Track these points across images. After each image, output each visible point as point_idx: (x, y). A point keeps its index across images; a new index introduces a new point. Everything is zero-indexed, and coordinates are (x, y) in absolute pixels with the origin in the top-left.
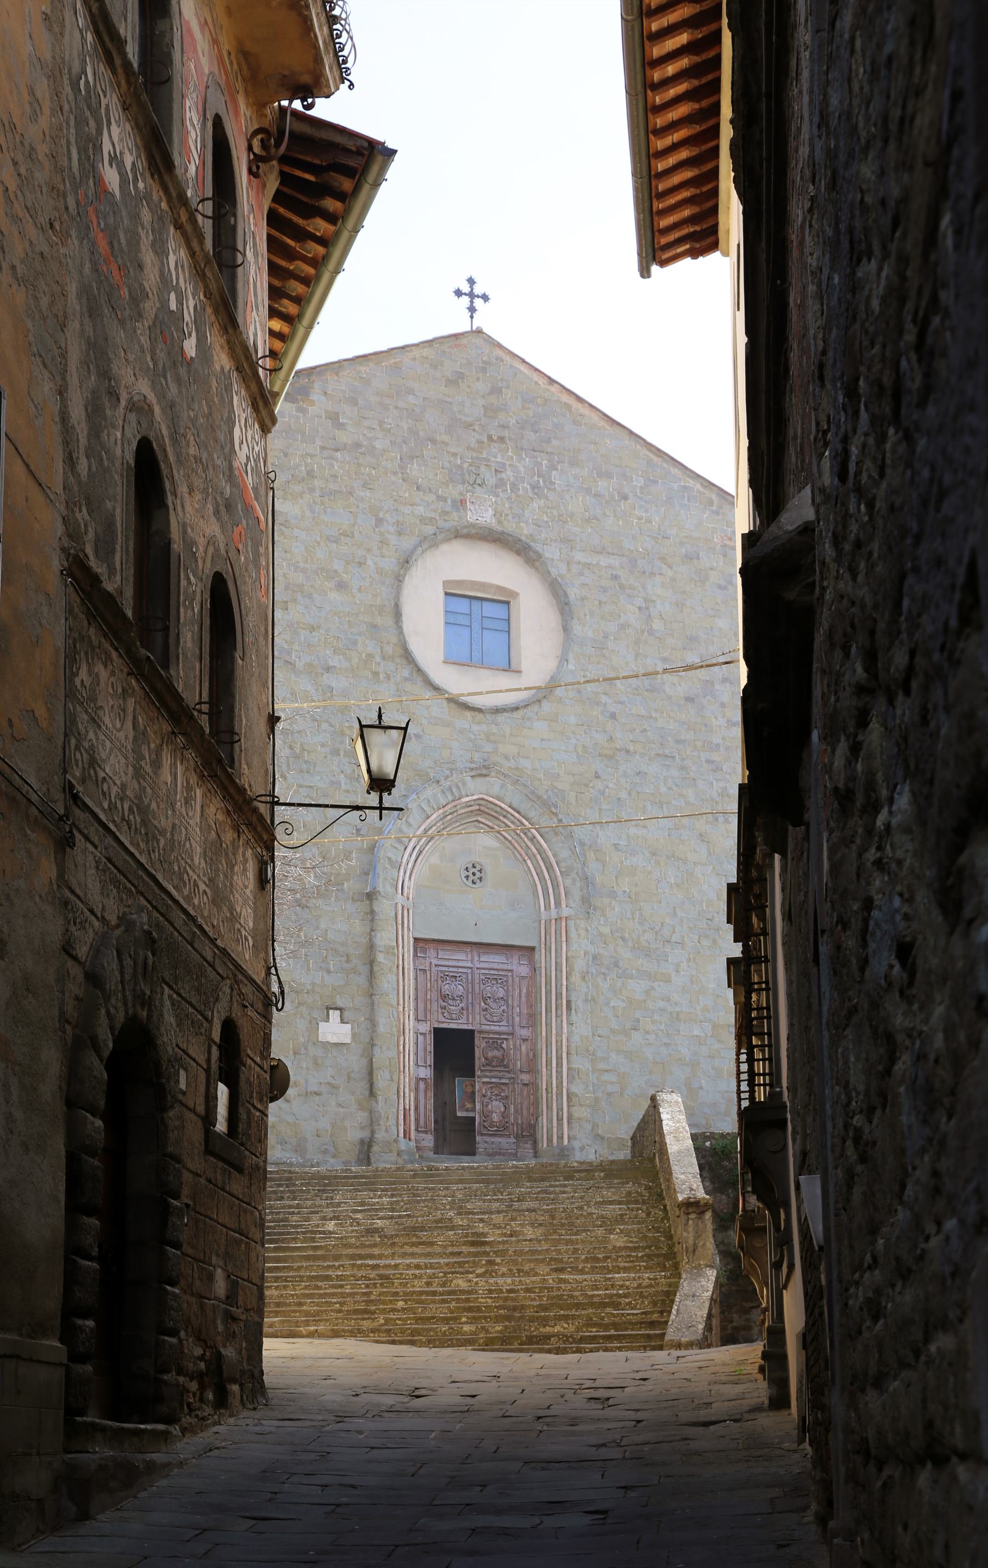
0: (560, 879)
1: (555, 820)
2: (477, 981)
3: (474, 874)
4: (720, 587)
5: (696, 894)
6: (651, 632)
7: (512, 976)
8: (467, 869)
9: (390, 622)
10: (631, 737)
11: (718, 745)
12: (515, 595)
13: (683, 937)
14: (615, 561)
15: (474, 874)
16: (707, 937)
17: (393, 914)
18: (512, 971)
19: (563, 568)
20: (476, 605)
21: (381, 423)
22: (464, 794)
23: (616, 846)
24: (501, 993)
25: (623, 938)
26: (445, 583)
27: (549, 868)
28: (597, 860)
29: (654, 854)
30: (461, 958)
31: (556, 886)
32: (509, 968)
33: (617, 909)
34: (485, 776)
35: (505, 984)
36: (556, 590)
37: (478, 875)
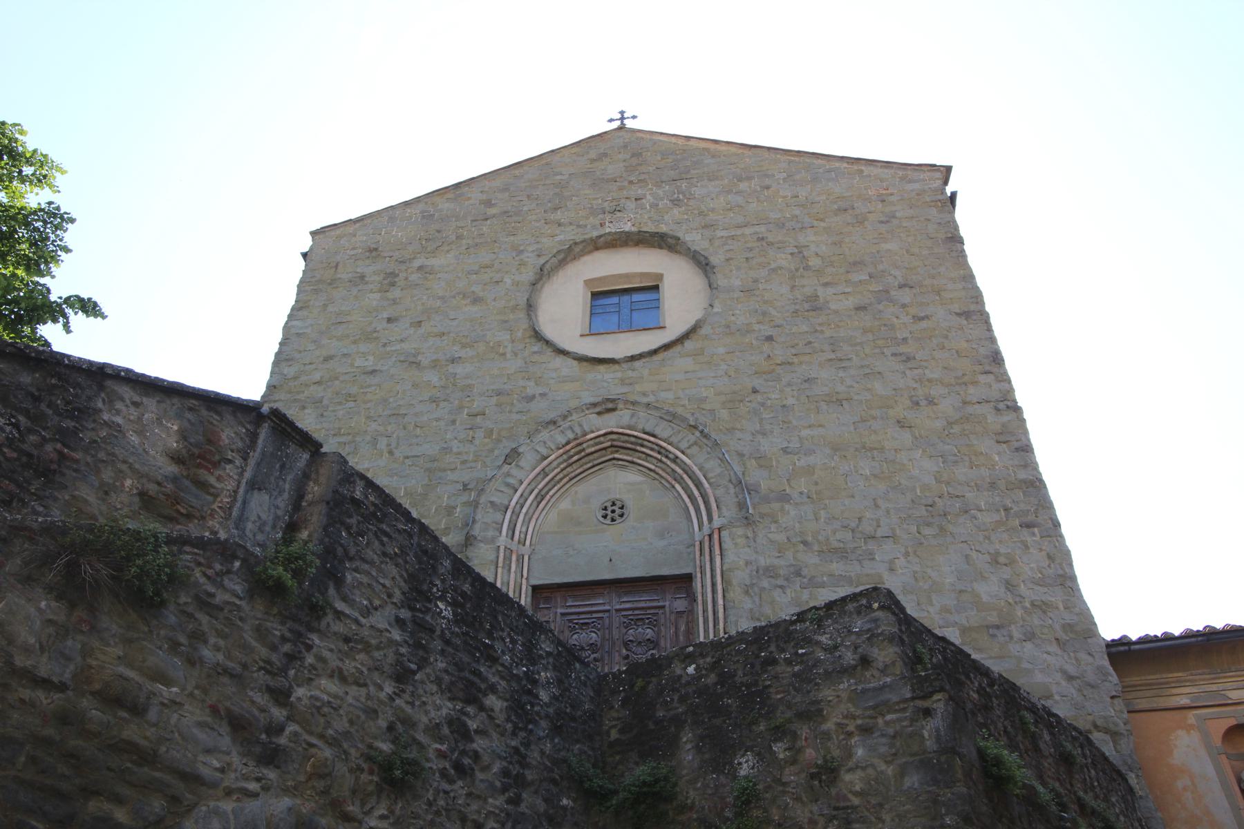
0: (709, 491)
1: (698, 434)
2: (615, 625)
3: (614, 512)
4: (882, 222)
5: (903, 481)
6: (807, 268)
7: (664, 613)
8: (605, 509)
9: (522, 315)
10: (794, 351)
11: (905, 340)
12: (660, 277)
13: (893, 530)
14: (762, 229)
15: (614, 512)
16: (928, 525)
17: (493, 557)
18: (663, 607)
19: (706, 244)
20: (626, 299)
21: (528, 196)
22: (587, 429)
23: (785, 451)
24: (649, 633)
25: (805, 543)
26: (588, 283)
27: (698, 485)
28: (761, 466)
29: (836, 449)
30: (601, 602)
31: (706, 503)
32: (661, 604)
33: (793, 513)
34: (613, 410)
35: (654, 624)
36: (703, 264)
37: (618, 511)
